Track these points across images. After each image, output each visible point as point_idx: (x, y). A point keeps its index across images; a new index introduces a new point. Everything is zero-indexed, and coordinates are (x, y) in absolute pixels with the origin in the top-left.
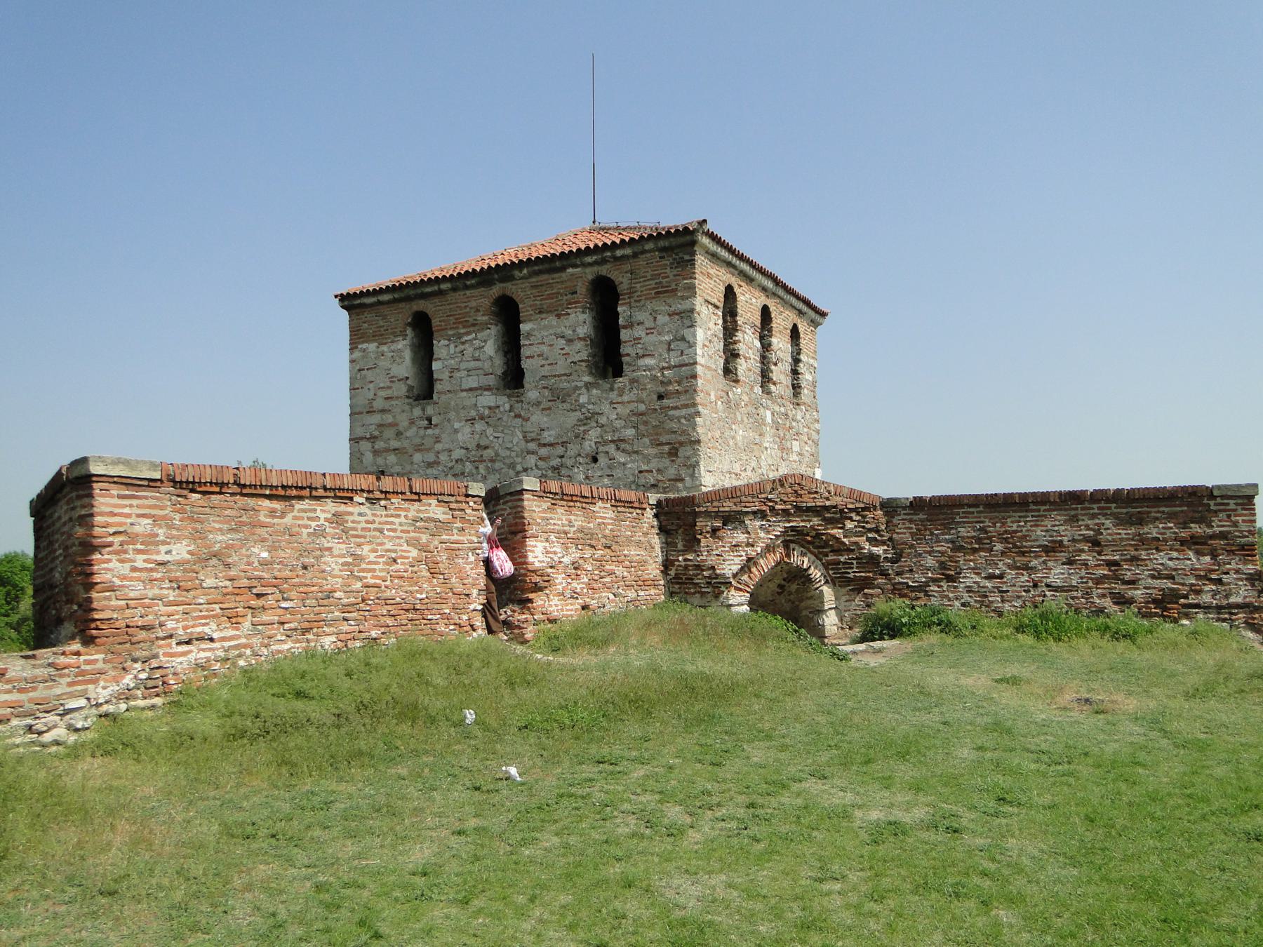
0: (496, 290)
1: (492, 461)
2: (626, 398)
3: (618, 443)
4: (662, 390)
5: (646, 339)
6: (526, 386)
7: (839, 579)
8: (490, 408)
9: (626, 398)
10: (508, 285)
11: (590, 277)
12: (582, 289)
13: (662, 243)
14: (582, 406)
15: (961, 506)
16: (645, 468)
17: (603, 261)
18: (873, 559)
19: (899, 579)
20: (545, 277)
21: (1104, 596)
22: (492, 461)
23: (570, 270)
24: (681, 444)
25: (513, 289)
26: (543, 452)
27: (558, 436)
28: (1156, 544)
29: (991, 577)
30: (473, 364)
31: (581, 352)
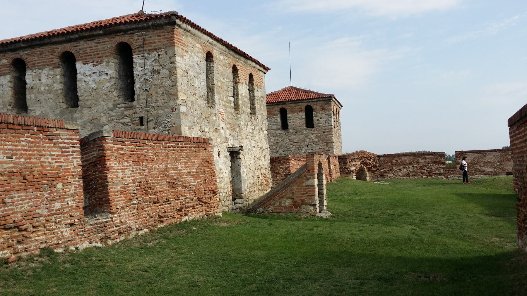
0: (281, 106)
1: (281, 146)
2: (315, 132)
3: (313, 142)
4: (324, 131)
5: (320, 120)
6: (289, 129)
7: (369, 171)
8: (279, 134)
9: (315, 132)
10: (284, 105)
11: (306, 105)
12: (304, 108)
13: (324, 99)
14: (304, 134)
15: (393, 156)
16: (320, 148)
17: (309, 102)
18: (376, 166)
19: (381, 170)
20: (294, 104)
21: (419, 172)
22: (281, 146)
23: (300, 103)
24: (329, 143)
25: (286, 107)
26: (294, 144)
27: (298, 141)
28: (429, 163)
29: (399, 169)
30: (274, 123)
31: (304, 122)
